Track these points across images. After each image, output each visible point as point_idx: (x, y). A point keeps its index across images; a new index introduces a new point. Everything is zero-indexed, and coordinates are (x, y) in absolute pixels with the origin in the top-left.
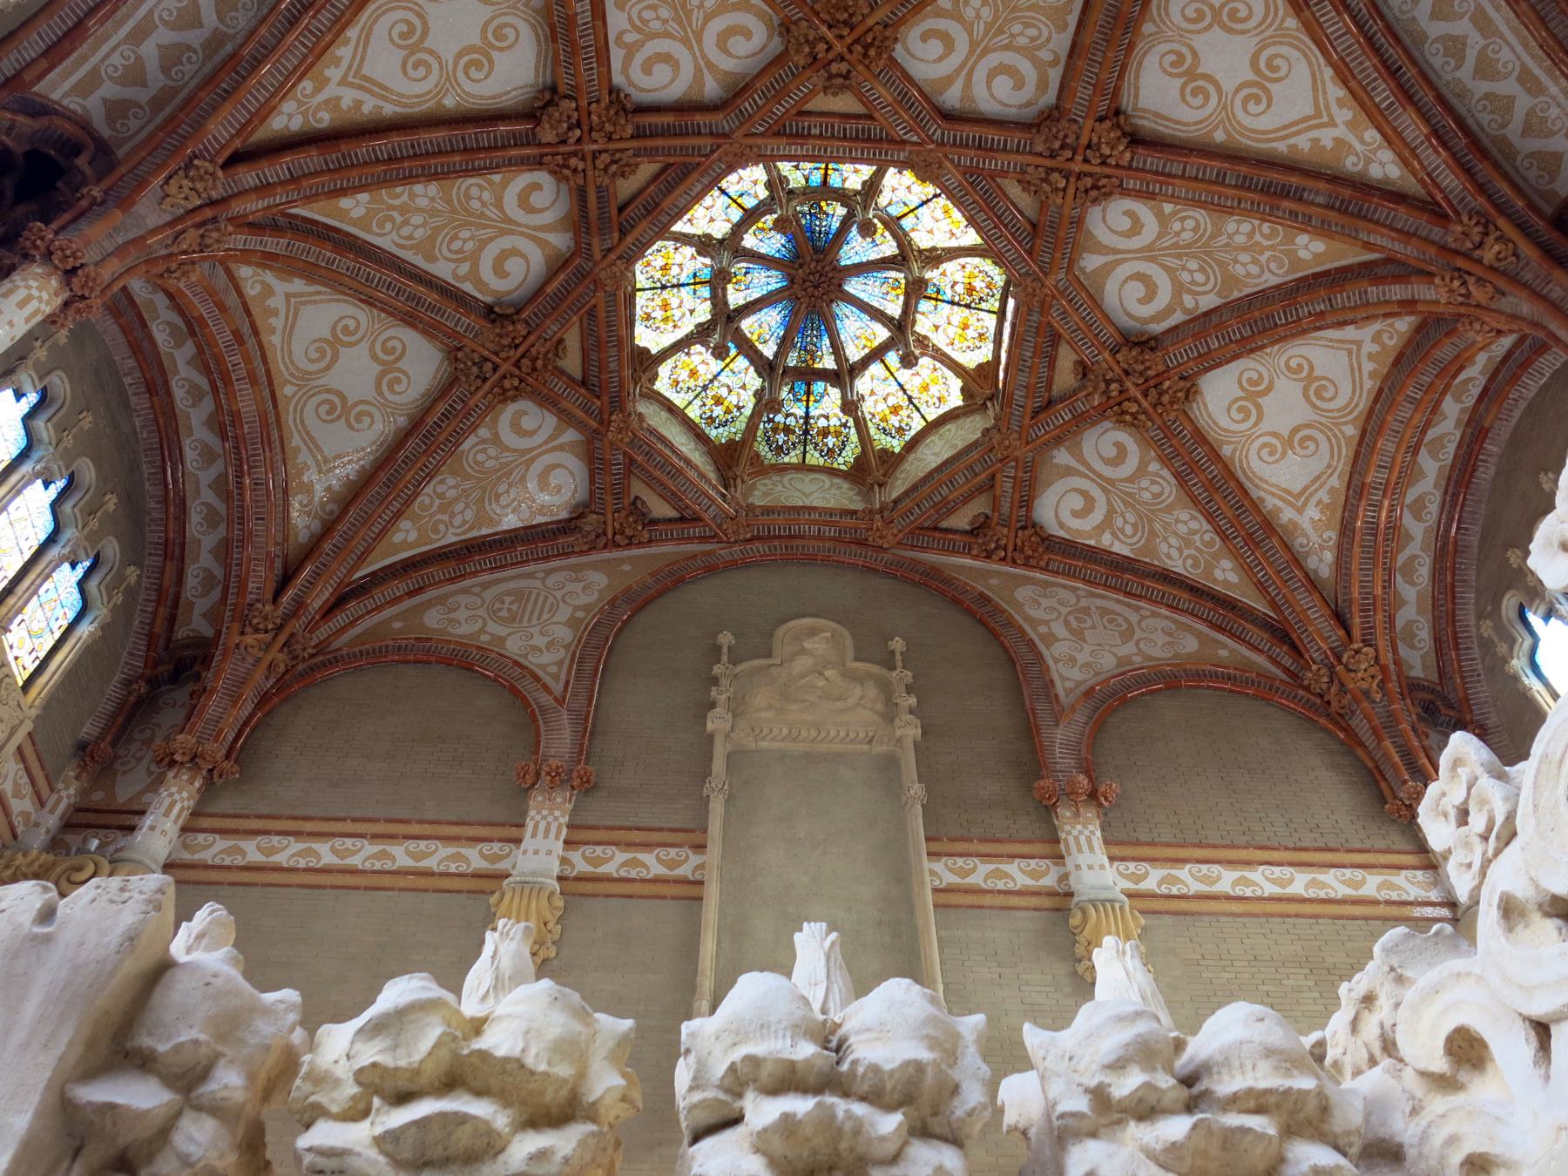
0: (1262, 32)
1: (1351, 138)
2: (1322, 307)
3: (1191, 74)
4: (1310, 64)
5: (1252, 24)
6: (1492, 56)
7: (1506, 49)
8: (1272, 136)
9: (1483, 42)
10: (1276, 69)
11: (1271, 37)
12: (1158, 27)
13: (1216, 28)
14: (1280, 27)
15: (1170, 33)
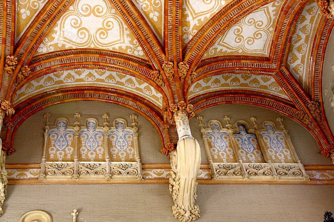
0: (94, 37)
1: (52, 43)
2: (8, 11)
3: (92, 11)
4: (79, 44)
5: (98, 36)
6: (51, 81)
7: (50, 84)
8: (63, 22)
9: (55, 81)
10: (82, 34)
11: (91, 38)
12: (111, 14)
13: (102, 27)
14: (93, 42)
15: (108, 15)
